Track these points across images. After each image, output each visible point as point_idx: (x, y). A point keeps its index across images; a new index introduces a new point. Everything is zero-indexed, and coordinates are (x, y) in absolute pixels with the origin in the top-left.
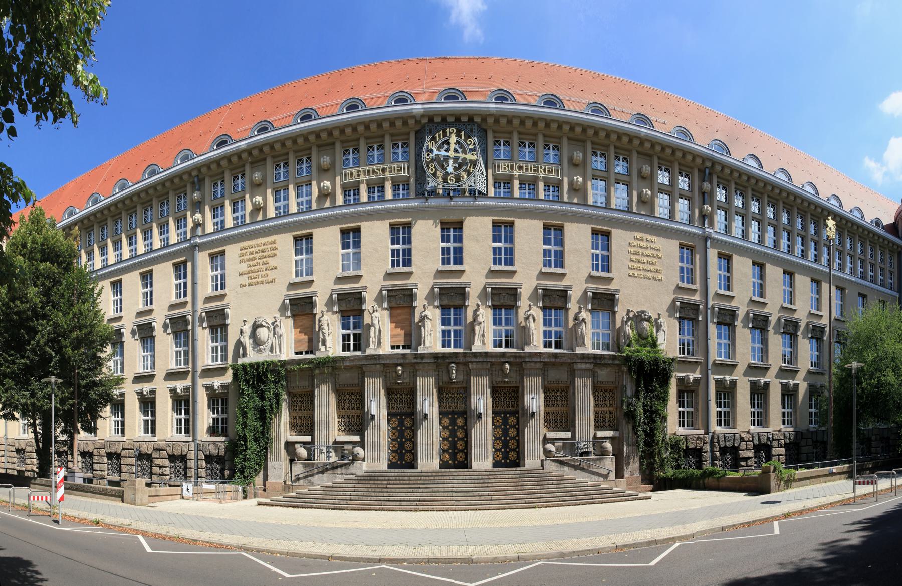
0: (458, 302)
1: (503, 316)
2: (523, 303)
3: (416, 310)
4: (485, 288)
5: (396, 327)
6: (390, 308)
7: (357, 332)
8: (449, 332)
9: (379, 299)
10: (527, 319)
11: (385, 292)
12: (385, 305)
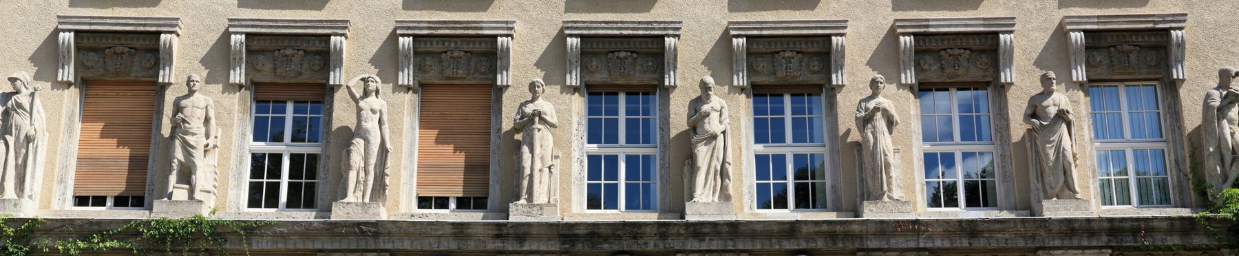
0: (639, 77)
2: (853, 78)
3: (507, 96)
5: (438, 141)
6: (422, 88)
7: (305, 149)
8: (612, 161)
10: (866, 121)
12: (406, 77)
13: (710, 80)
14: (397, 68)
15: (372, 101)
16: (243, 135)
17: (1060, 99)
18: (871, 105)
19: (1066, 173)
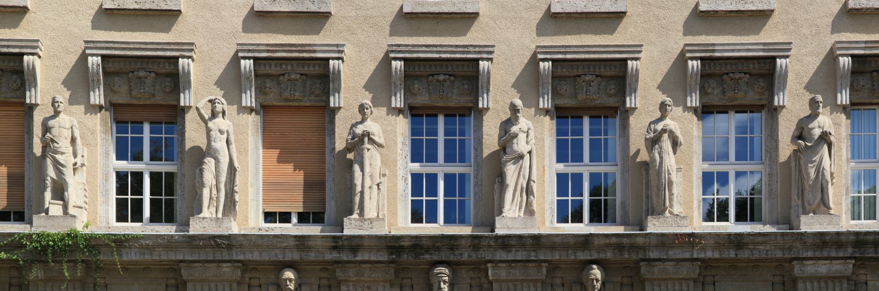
0: (456, 99)
1: (586, 138)
2: (645, 101)
3: (339, 117)
4: (534, 61)
5: (280, 160)
6: (264, 109)
7: (162, 167)
8: (432, 179)
9: (231, 81)
10: (654, 142)
11: (247, 65)
12: (249, 99)
13: (519, 103)
14: (241, 91)
15: (219, 120)
16: (107, 154)
17: (825, 121)
18: (660, 126)
19: (824, 190)
